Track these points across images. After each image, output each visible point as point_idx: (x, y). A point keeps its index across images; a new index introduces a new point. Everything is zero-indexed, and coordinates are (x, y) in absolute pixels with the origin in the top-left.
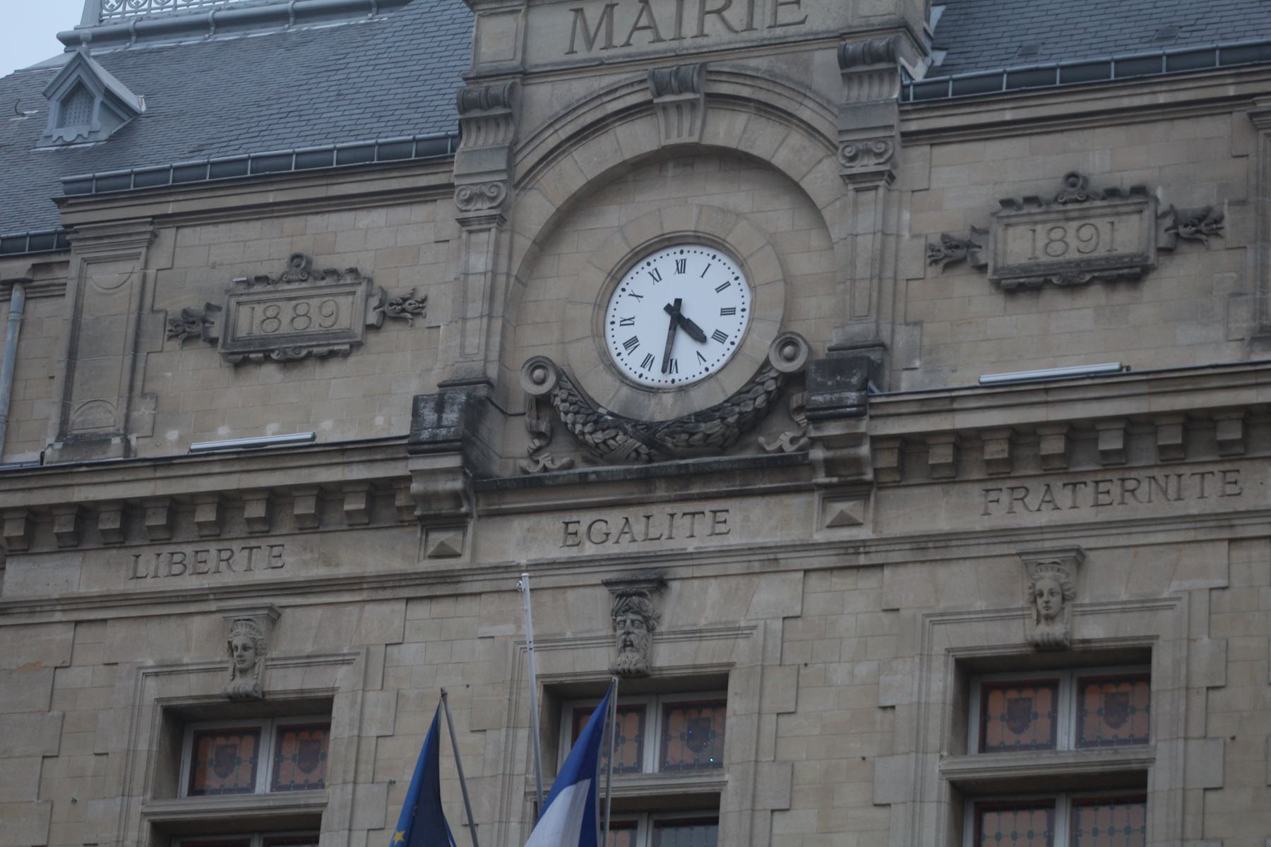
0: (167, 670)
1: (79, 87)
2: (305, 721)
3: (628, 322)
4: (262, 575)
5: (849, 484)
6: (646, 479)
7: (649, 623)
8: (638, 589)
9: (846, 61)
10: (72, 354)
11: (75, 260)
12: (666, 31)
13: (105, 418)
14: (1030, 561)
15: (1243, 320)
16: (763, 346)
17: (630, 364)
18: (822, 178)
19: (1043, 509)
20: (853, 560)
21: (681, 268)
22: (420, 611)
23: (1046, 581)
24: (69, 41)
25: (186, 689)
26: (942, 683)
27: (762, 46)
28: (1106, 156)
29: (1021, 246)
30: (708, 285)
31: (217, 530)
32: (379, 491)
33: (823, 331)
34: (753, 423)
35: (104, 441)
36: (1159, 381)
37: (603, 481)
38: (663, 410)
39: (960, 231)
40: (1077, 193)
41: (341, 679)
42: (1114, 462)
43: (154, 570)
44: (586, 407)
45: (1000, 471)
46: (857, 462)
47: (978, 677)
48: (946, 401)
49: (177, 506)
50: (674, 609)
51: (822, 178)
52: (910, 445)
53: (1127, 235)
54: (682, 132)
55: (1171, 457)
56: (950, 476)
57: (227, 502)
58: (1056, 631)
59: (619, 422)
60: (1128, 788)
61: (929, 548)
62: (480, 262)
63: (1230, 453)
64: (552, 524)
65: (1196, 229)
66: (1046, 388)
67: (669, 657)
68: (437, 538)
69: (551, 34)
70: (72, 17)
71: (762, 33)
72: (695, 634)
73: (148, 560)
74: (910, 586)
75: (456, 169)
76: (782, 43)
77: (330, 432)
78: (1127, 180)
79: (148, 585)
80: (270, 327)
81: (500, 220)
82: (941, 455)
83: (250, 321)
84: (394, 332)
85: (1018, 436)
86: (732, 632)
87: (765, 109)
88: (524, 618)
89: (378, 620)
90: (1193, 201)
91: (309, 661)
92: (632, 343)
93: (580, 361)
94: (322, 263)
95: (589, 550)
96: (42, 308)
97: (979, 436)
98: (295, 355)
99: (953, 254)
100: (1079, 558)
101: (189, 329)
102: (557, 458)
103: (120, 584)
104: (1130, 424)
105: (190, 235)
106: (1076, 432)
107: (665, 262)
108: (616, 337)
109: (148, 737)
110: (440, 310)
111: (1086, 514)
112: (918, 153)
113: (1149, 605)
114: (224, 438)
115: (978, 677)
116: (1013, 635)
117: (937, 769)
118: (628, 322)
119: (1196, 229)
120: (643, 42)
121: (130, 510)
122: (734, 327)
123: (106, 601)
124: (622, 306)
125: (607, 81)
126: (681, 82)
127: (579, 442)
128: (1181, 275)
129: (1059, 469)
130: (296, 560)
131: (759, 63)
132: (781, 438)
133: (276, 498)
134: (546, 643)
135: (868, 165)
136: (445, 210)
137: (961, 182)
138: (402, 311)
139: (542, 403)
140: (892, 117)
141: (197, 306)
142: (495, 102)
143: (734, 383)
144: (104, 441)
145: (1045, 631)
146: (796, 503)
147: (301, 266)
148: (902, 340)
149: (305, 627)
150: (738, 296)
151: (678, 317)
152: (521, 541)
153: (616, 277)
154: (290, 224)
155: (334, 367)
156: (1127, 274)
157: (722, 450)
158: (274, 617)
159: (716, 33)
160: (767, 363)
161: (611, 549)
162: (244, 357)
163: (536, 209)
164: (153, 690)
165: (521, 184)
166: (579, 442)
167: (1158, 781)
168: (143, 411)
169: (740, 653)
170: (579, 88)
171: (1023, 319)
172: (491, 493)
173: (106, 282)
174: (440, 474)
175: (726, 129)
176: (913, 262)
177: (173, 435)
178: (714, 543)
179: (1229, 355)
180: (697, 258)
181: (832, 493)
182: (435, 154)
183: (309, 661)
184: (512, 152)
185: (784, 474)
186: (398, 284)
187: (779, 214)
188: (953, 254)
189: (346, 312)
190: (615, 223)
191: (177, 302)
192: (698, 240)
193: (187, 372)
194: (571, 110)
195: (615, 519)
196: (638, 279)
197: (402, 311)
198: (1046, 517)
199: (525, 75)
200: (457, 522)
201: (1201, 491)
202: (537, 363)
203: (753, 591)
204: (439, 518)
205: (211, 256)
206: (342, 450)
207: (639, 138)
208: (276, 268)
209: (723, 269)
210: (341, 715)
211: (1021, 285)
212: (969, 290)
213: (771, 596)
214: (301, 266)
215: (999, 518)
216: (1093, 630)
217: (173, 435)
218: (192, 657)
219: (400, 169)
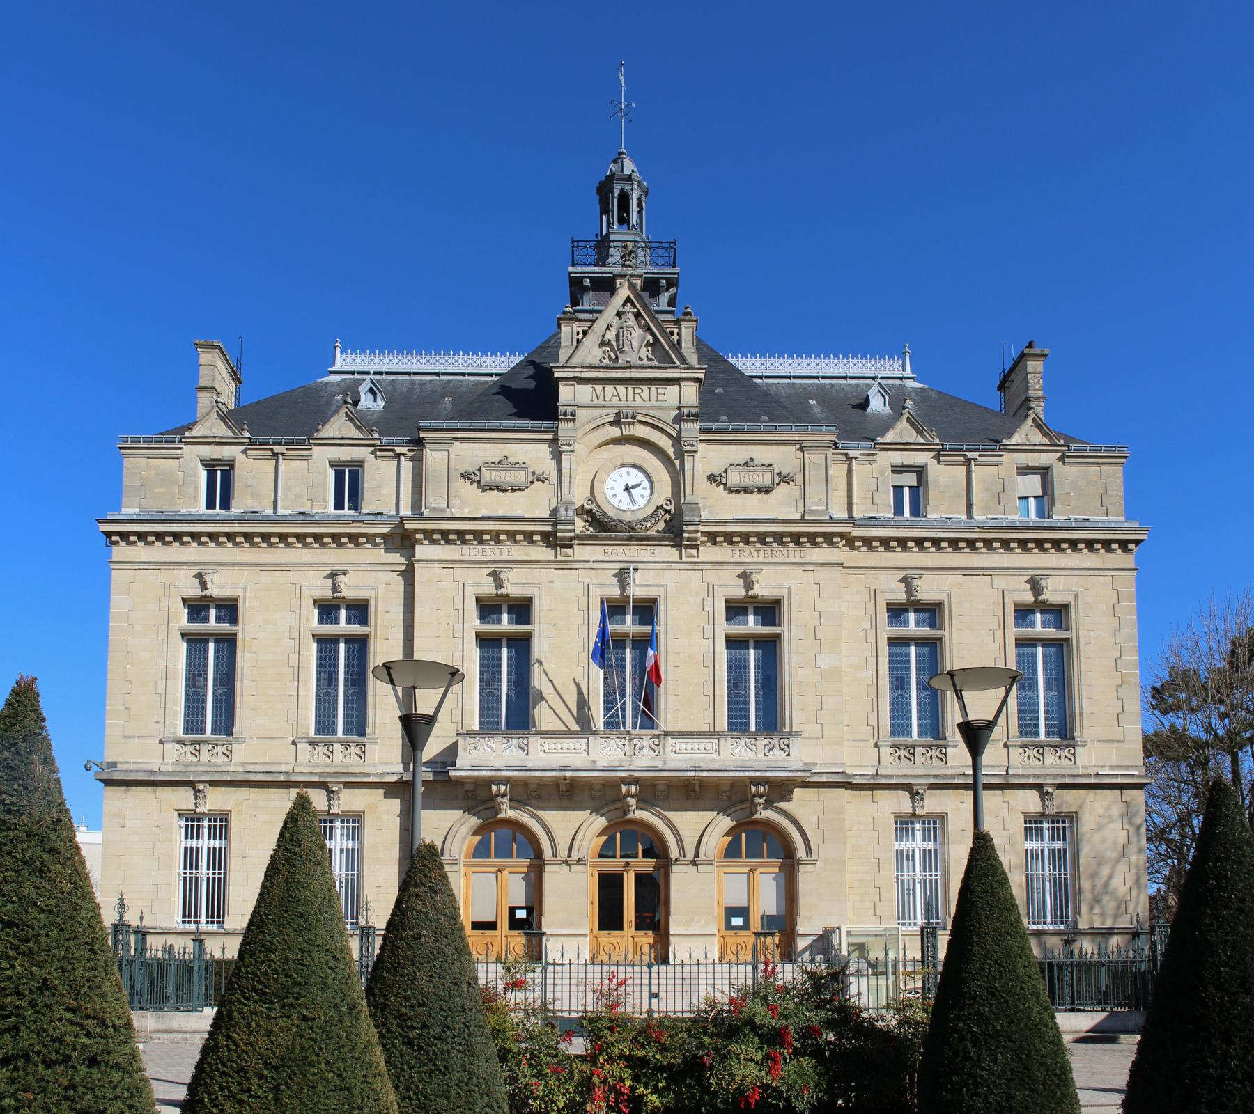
3: (613, 489)
6: (630, 539)
12: (623, 398)
17: (615, 502)
20: (695, 567)
21: (629, 474)
28: (761, 453)
29: (734, 478)
35: (444, 510)
37: (616, 538)
39: (717, 473)
46: (696, 539)
52: (712, 537)
53: (765, 479)
54: (628, 431)
71: (654, 402)
74: (711, 576)
77: (519, 513)
80: (498, 479)
83: (488, 476)
88: (587, 576)
92: (614, 495)
95: (612, 558)
101: (466, 476)
111: (762, 559)
113: (780, 586)
118: (613, 489)
119: (785, 479)
120: (615, 400)
125: (605, 411)
131: (651, 412)
139: (590, 512)
140: (696, 434)
141: (471, 470)
154: (500, 445)
159: (639, 401)
161: (619, 559)
177: (466, 510)
178: (652, 559)
195: (620, 549)
207: (615, 432)
215: (736, 559)
217: (466, 510)
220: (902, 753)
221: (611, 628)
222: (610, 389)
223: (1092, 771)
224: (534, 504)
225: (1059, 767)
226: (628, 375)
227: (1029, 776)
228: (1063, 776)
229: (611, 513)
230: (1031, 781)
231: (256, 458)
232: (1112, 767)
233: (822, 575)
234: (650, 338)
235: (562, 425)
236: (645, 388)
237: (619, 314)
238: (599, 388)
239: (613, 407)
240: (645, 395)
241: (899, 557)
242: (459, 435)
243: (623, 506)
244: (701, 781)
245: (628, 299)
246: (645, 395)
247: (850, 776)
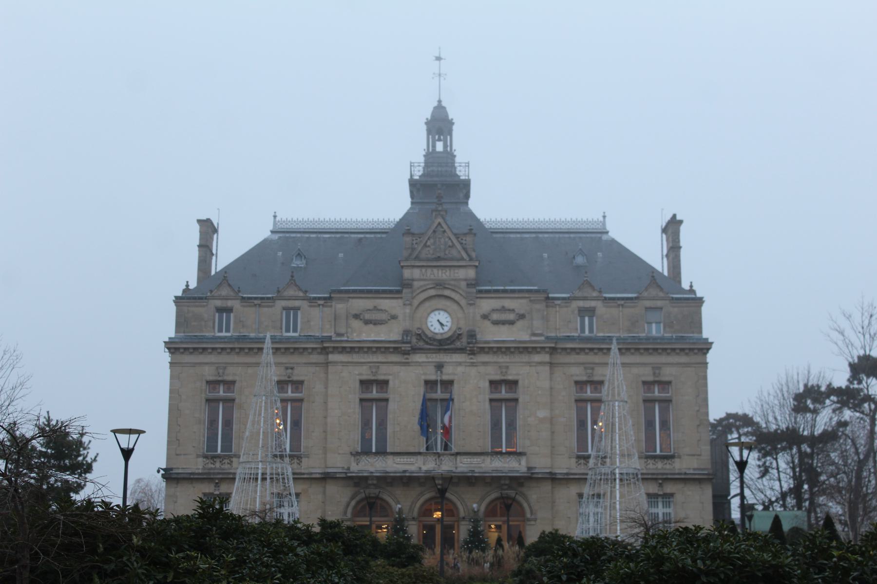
0: (360, 374)
1: (299, 254)
2: (383, 384)
4: (375, 360)
5: (472, 353)
6: (440, 350)
7: (441, 372)
8: (440, 367)
9: (468, 285)
10: (335, 319)
11: (333, 303)
13: (342, 330)
14: (500, 367)
15: (529, 332)
16: (454, 329)
17: (432, 329)
18: (463, 302)
19: (502, 359)
20: (473, 364)
22: (403, 368)
23: (504, 370)
24: (272, 232)
25: (364, 377)
26: (487, 384)
27: (453, 280)
28: (508, 303)
29: (495, 316)
30: (444, 317)
31: (366, 352)
32: (395, 348)
33: (465, 329)
34: (454, 341)
35: (342, 335)
36: (520, 342)
38: (439, 337)
40: (503, 309)
41: (390, 378)
42: (512, 353)
43: (356, 358)
44: (426, 336)
45: (495, 353)
47: (492, 382)
48: (488, 342)
49: (360, 348)
50: (444, 370)
51: (463, 302)
52: (482, 349)
53: (511, 317)
54: (440, 292)
55: (521, 353)
56: (488, 353)
57: (369, 348)
58: (505, 378)
59: (435, 340)
60: (516, 400)
61: (485, 364)
62: (408, 311)
63: (530, 353)
64: (424, 355)
65: (522, 317)
66: (503, 342)
67: (445, 378)
68: (406, 356)
69: (416, 273)
70: (271, 228)
72: (449, 374)
73: (355, 356)
74: (482, 369)
75: (403, 295)
76: (455, 280)
78: (511, 308)
79: (355, 360)
81: (410, 304)
82: (486, 350)
83: (367, 316)
84: (393, 321)
85: (498, 348)
86: (454, 374)
87: (453, 290)
89: (396, 368)
90: (522, 312)
91: (385, 374)
93: (424, 327)
94: (379, 308)
96: (326, 309)
97: (492, 348)
98: (376, 323)
99: (485, 317)
100: (507, 367)
101: (356, 316)
102: (421, 344)
103: (350, 360)
104: (515, 348)
105: (354, 300)
106: (508, 348)
107: (437, 312)
108: (429, 324)
109: (358, 384)
110: (401, 318)
111: (508, 360)
112: (478, 300)
113: (518, 374)
114: (364, 337)
115: (492, 382)
116: (498, 377)
117: (487, 397)
119: (522, 317)
120: (432, 277)
121: (352, 348)
122: (449, 324)
123: (349, 362)
124: (430, 319)
125: (427, 282)
126: (440, 284)
127: (424, 341)
128: (520, 324)
129: (503, 353)
130: (380, 358)
131: (452, 282)
132: (458, 344)
133: (377, 348)
134: (425, 374)
135: (472, 302)
136: (400, 301)
137: (486, 305)
138: (394, 317)
139: (419, 335)
141: (357, 313)
142: (408, 284)
143: (450, 334)
144: (342, 335)
145: (503, 378)
146: (463, 355)
147: (376, 309)
148: (477, 330)
149: (384, 369)
150: (449, 319)
151: (439, 322)
152: (419, 358)
153: (429, 314)
154: (373, 300)
155: (383, 326)
156: (512, 323)
157: (449, 344)
158: (378, 367)
159: (444, 277)
160: (455, 332)
161: (434, 360)
162: (367, 322)
163: (416, 302)
164: (358, 378)
165: (413, 298)
166: (424, 341)
167: (520, 400)
168: (349, 330)
169: (456, 378)
170: (422, 283)
171: (495, 328)
172: (415, 350)
173: (340, 307)
174: (406, 347)
175: (447, 293)
176: (478, 317)
179: (526, 338)
180: (442, 313)
181: (469, 354)
182: (399, 292)
183: (385, 374)
184: (412, 293)
185: (461, 350)
186: (394, 312)
187: (455, 307)
188: (485, 317)
189: (384, 316)
190: (427, 304)
191: (354, 312)
192: (445, 311)
193: (356, 324)
194: (421, 286)
195: (434, 355)
196: (432, 315)
197: (394, 317)
198: (502, 360)
199: (413, 280)
200: (409, 354)
201: (525, 358)
202: (419, 328)
203: (456, 367)
204: (406, 353)
205: (359, 304)
206: (390, 342)
207: (432, 292)
208: (371, 308)
209: (446, 315)
210: (391, 382)
211: (496, 323)
212: (487, 323)
213: (460, 369)
214: (376, 309)
216: (510, 378)
218: (366, 373)
219: (395, 294)
220: (582, 461)
221: (429, 396)
222: (429, 271)
223: (683, 471)
224: (390, 333)
225: (665, 469)
226: (438, 264)
227: (648, 474)
228: (667, 474)
229: (430, 335)
230: (649, 476)
231: (244, 306)
232: (694, 469)
233: (540, 368)
234: (450, 244)
235: (405, 291)
236: (448, 270)
237: (434, 232)
238: (424, 270)
239: (430, 280)
240: (448, 274)
241: (582, 358)
242: (351, 295)
243: (437, 331)
244: (476, 477)
245: (439, 224)
246: (448, 274)
247: (555, 474)
